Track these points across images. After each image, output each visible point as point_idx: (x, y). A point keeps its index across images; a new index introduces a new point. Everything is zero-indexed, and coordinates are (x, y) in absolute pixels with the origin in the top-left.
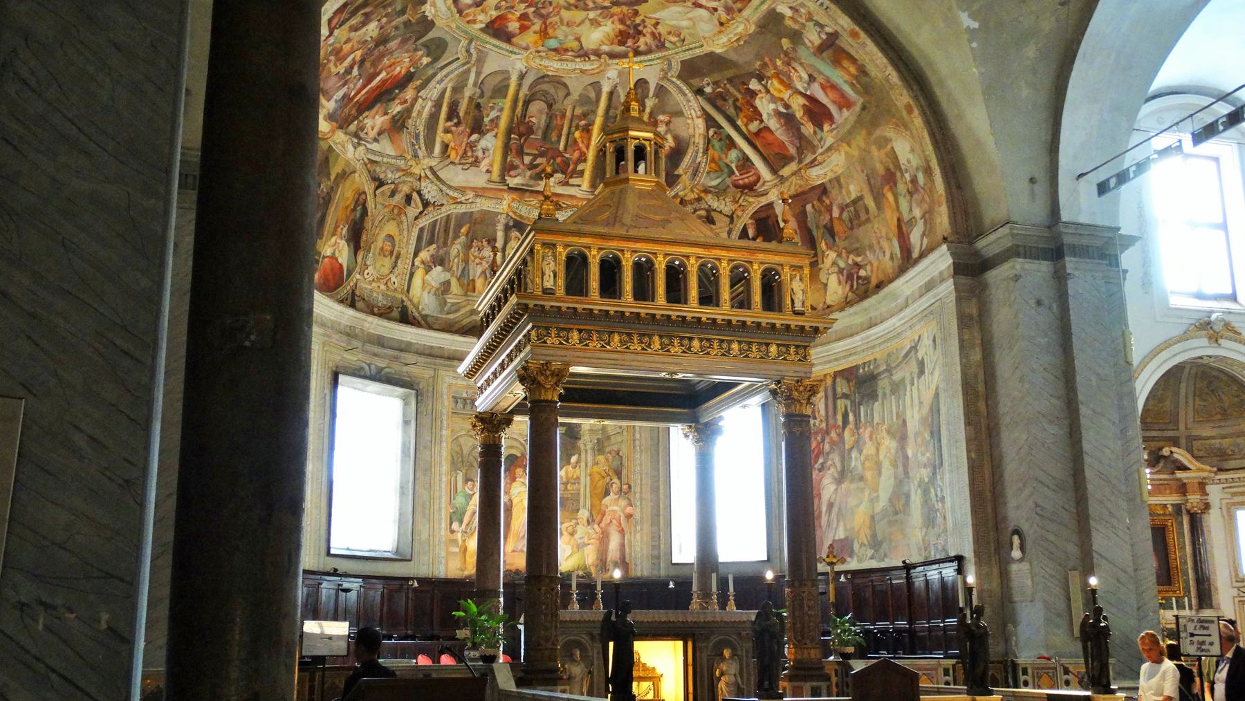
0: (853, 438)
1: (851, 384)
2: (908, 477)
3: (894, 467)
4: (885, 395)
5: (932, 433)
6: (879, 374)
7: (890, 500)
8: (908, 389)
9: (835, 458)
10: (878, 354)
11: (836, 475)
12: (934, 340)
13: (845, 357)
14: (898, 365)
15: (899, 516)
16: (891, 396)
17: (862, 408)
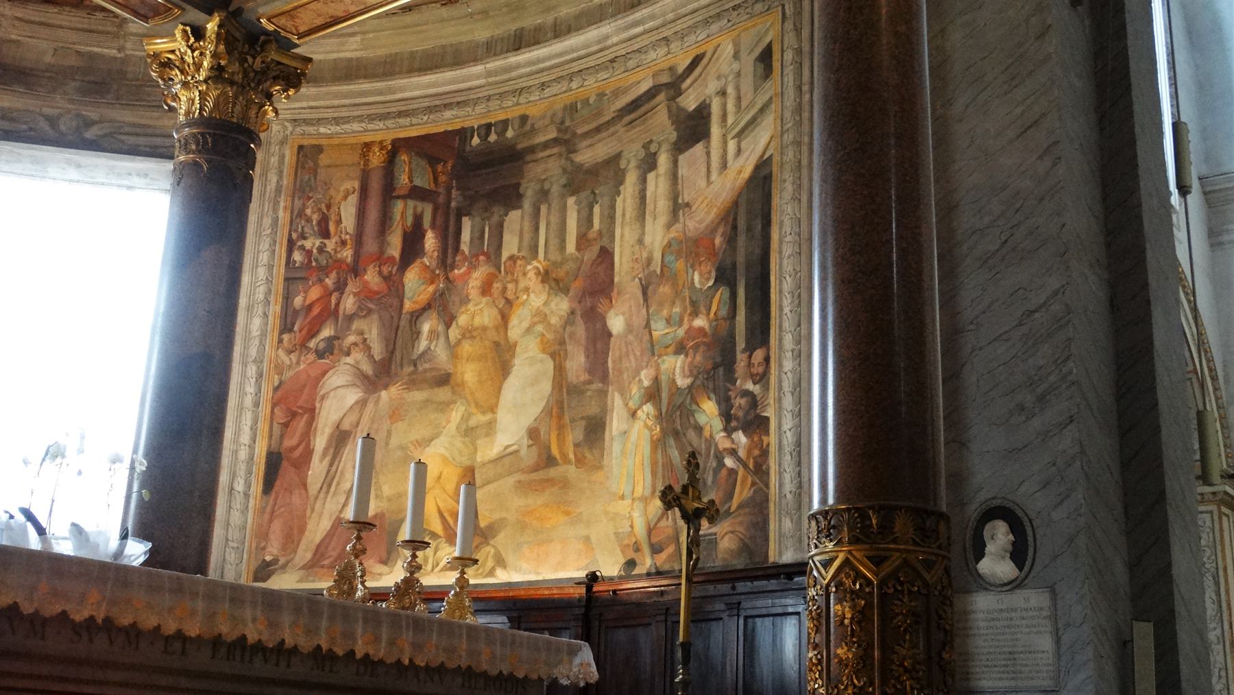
0: (431, 289)
1: (440, 168)
2: (604, 378)
3: (553, 355)
4: (544, 194)
5: (725, 277)
6: (532, 150)
7: (533, 433)
8: (631, 178)
9: (373, 331)
10: (535, 106)
11: (367, 368)
12: (766, 57)
13: (430, 110)
14: (598, 130)
15: (553, 472)
16: (563, 197)
17: (467, 224)
